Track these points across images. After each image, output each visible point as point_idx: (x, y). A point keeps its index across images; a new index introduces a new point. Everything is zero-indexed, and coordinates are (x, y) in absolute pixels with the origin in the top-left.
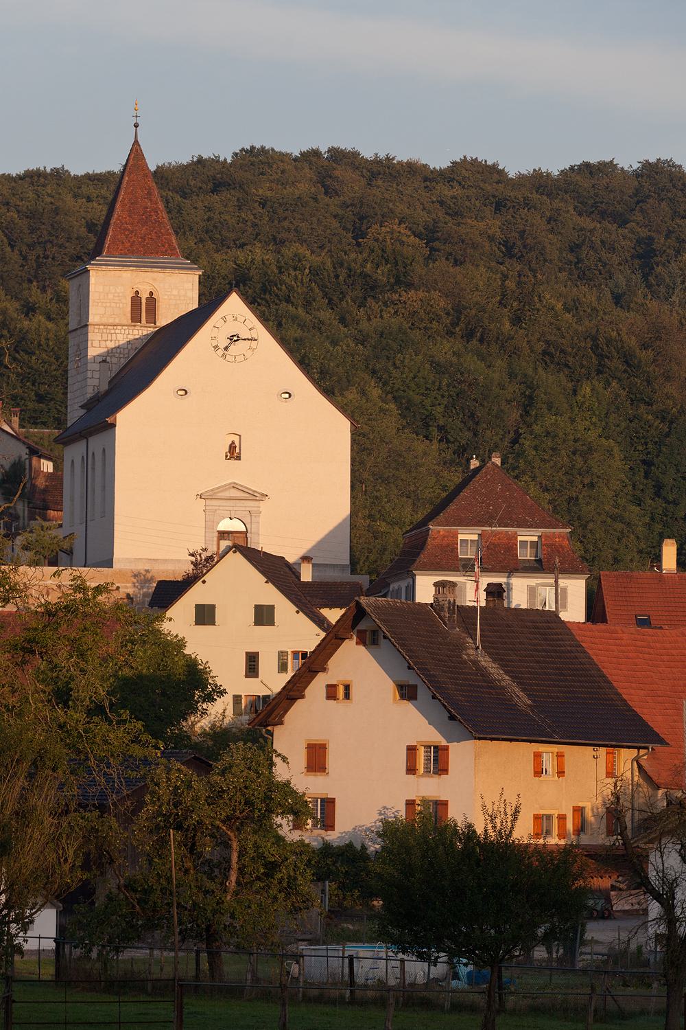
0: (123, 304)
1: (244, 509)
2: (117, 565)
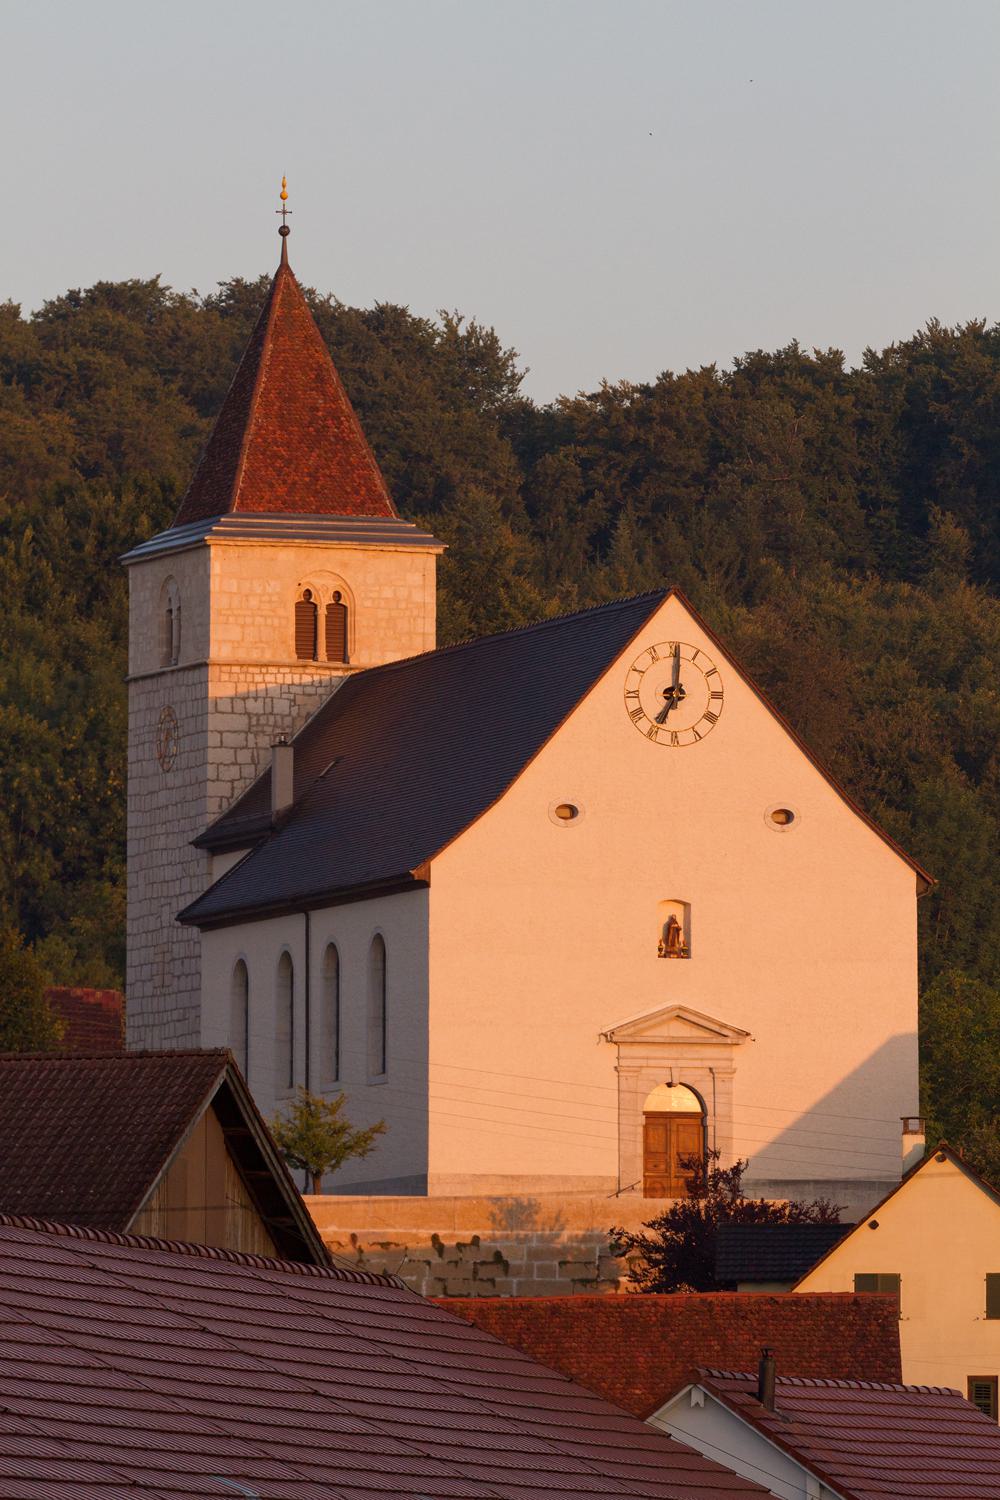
0: (280, 618)
1: (697, 1063)
2: (433, 1190)
